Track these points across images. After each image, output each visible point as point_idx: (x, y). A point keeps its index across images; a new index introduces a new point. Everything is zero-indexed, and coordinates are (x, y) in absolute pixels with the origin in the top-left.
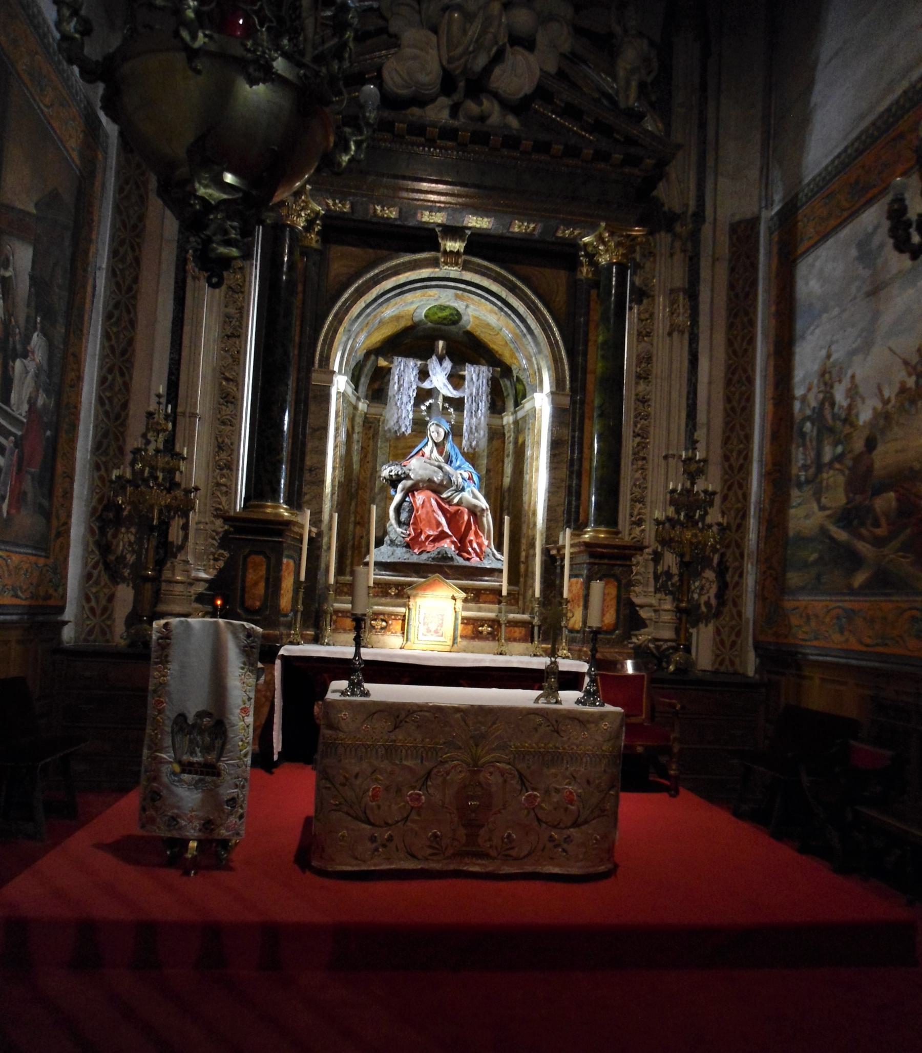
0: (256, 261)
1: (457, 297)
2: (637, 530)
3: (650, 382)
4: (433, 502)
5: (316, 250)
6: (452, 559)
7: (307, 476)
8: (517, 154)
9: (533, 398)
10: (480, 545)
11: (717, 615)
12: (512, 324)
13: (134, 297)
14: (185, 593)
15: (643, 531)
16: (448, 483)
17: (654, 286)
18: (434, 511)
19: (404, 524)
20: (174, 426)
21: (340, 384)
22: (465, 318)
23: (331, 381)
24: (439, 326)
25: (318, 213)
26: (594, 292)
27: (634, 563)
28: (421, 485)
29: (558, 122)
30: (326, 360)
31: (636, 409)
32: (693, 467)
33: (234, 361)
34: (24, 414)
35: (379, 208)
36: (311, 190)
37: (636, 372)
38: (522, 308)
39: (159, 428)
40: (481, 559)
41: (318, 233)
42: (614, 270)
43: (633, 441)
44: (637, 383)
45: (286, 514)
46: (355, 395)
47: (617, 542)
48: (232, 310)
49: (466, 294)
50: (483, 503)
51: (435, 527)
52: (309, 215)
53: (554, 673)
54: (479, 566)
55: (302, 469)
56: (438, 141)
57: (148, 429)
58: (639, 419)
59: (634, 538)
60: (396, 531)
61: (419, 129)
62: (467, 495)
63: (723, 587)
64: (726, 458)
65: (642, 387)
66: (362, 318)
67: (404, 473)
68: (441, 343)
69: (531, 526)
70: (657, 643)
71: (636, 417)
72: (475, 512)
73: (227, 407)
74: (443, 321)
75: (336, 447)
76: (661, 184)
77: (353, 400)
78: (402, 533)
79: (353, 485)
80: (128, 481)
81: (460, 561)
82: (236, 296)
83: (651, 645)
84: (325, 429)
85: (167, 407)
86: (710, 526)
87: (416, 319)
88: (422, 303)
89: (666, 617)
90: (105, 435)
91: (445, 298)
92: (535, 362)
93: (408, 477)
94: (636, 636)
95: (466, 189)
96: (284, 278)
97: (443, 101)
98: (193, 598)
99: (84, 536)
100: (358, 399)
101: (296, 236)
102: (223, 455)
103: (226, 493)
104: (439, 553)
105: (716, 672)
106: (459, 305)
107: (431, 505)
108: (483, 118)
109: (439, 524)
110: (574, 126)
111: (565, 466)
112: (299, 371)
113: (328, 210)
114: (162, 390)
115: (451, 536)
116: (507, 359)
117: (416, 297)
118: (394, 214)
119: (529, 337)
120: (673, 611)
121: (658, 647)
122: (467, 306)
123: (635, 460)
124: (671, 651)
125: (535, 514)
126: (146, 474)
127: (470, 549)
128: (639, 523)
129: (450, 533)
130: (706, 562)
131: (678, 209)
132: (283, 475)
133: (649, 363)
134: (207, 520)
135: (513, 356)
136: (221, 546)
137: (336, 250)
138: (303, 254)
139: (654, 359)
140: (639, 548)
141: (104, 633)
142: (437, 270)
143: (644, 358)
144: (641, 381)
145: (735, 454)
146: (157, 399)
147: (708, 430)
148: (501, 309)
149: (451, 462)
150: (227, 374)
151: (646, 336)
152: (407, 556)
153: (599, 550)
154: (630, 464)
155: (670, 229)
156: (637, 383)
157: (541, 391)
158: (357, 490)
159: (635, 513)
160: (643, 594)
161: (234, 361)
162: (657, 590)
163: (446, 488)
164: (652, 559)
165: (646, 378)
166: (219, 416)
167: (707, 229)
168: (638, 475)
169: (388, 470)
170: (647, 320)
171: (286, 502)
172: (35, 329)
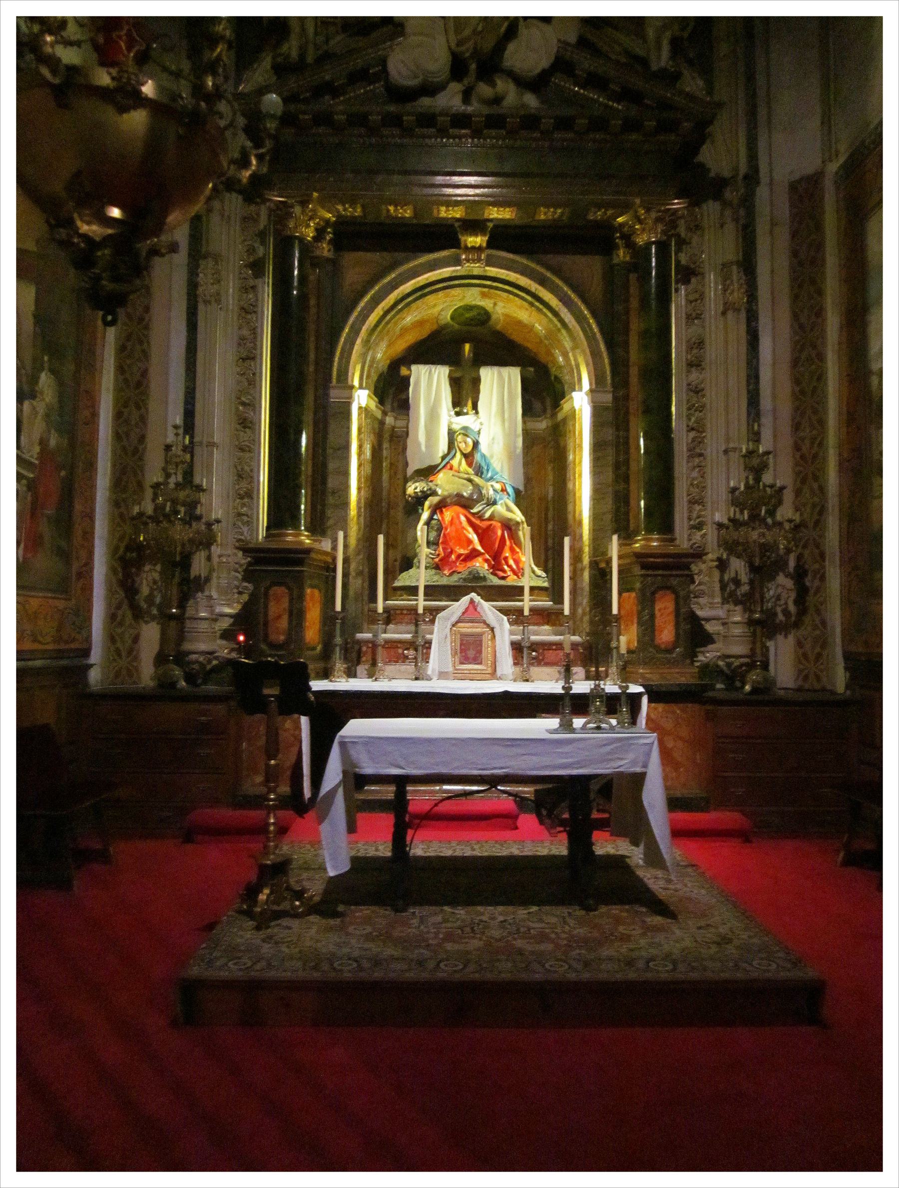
0: (269, 278)
1: (484, 295)
2: (698, 536)
3: (703, 369)
4: (463, 518)
5: (328, 260)
6: (484, 579)
7: (331, 500)
8: (537, 135)
9: (572, 398)
10: (517, 562)
11: (797, 625)
12: (545, 321)
13: (147, 327)
14: (209, 630)
15: (705, 534)
16: (479, 496)
17: (702, 262)
18: (463, 528)
20: (192, 457)
21: (362, 398)
22: (494, 317)
23: (350, 397)
24: (470, 328)
25: (327, 222)
26: (633, 277)
27: (696, 572)
28: (449, 501)
29: (582, 94)
30: (344, 375)
31: (688, 401)
32: (755, 462)
33: (250, 384)
34: (35, 456)
35: (391, 208)
36: (318, 197)
37: (687, 359)
38: (554, 302)
39: (178, 460)
40: (518, 577)
41: (330, 242)
42: (653, 250)
43: (687, 435)
44: (689, 372)
45: (308, 541)
46: (380, 409)
47: (671, 549)
48: (245, 332)
49: (492, 291)
50: (518, 515)
51: (465, 544)
52: (318, 223)
53: (601, 697)
54: (515, 584)
55: (324, 492)
56: (451, 130)
57: (167, 462)
58: (692, 411)
59: (695, 544)
61: (428, 120)
62: (500, 509)
63: (802, 593)
64: (797, 448)
65: (694, 376)
66: (381, 327)
67: (430, 489)
68: (467, 347)
69: (577, 538)
70: (728, 660)
71: (689, 409)
72: (509, 526)
73: (245, 432)
74: (470, 322)
75: (360, 466)
76: (705, 147)
77: (379, 414)
78: (431, 554)
80: (150, 517)
81: (496, 581)
82: (249, 317)
83: (721, 663)
84: (347, 447)
85: (184, 438)
86: (780, 524)
87: (443, 322)
88: (445, 304)
89: (737, 631)
90: (123, 472)
91: (472, 297)
92: (572, 358)
93: (434, 493)
94: (703, 653)
95: (500, 179)
96: (295, 292)
97: (455, 87)
98: (218, 634)
99: (106, 575)
100: (385, 413)
101: (306, 249)
102: (244, 484)
103: (248, 523)
104: (470, 573)
105: (799, 690)
106: (487, 304)
107: (461, 523)
108: (497, 100)
109: (470, 542)
110: (599, 97)
111: (610, 469)
112: (316, 390)
113: (339, 216)
114: (179, 420)
115: (483, 554)
116: (543, 357)
117: (439, 299)
118: (408, 213)
119: (564, 332)
120: (745, 623)
121: (729, 665)
122: (495, 304)
123: (691, 457)
124: (744, 668)
125: (580, 523)
126: (168, 509)
127: (506, 567)
128: (699, 527)
129: (482, 551)
130: (780, 565)
131: (726, 174)
132: (303, 500)
133: (700, 349)
134: (229, 552)
135: (549, 353)
136: (245, 579)
137: (350, 258)
138: (314, 265)
139: (707, 342)
140: (698, 554)
141: (130, 675)
142: (459, 268)
143: (695, 344)
144: (693, 369)
145: (807, 442)
146: (175, 431)
147: (775, 419)
148: (531, 304)
149: (482, 473)
150: (243, 399)
151: (696, 318)
152: (436, 578)
153: (652, 560)
154: (685, 461)
155: (717, 196)
156: (689, 372)
157: (581, 389)
158: (388, 510)
159: (694, 515)
160: (708, 605)
161: (250, 384)
162: (725, 601)
163: (477, 502)
164: (717, 567)
165: (698, 365)
166: (237, 443)
167: (762, 192)
168: (695, 474)
169: (413, 487)
170: (696, 300)
171: (307, 529)
172: (43, 370)
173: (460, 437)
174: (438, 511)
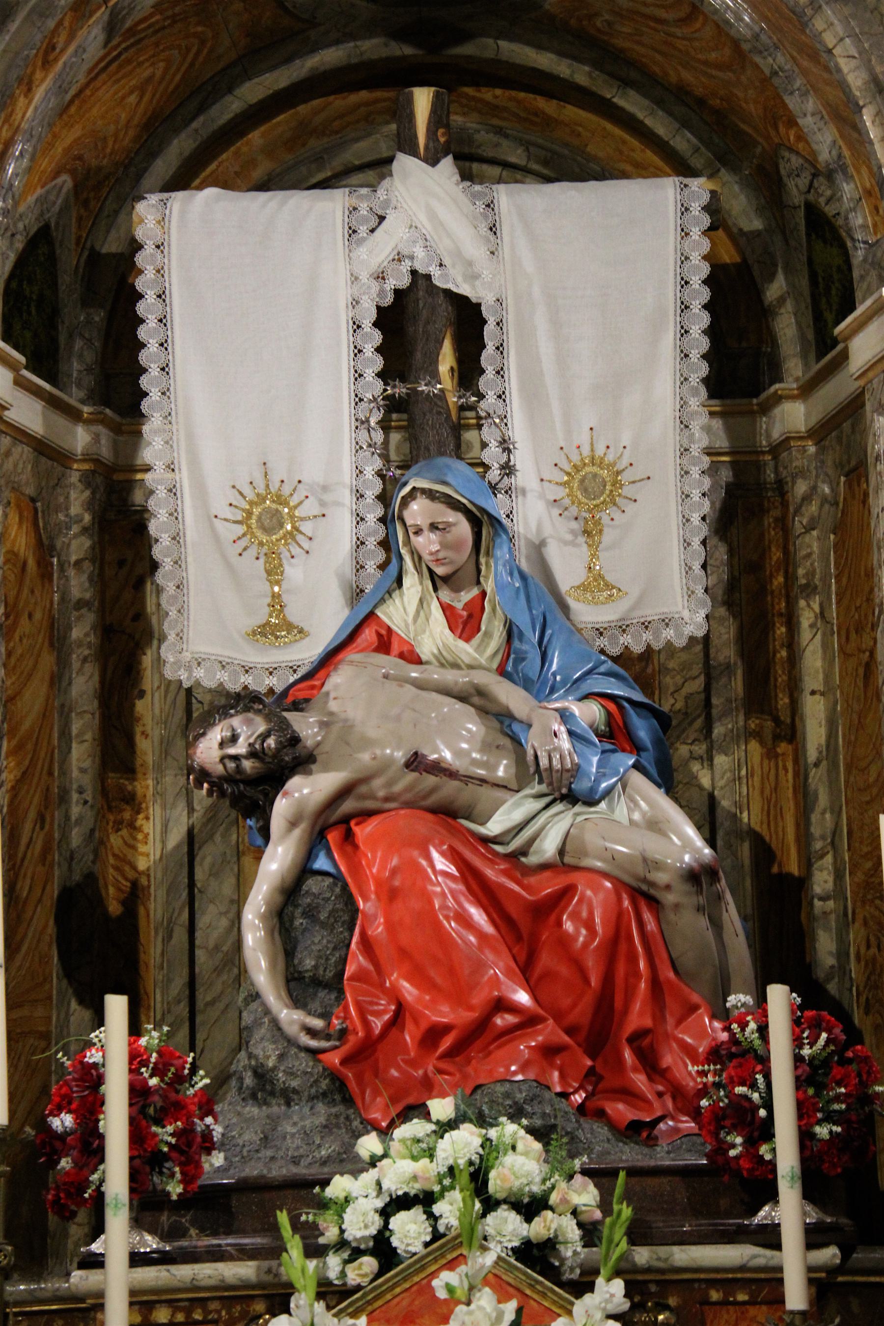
19: (317, 983)
60: (275, 1024)
79: (76, 810)
173: (415, 506)
174: (333, 837)
